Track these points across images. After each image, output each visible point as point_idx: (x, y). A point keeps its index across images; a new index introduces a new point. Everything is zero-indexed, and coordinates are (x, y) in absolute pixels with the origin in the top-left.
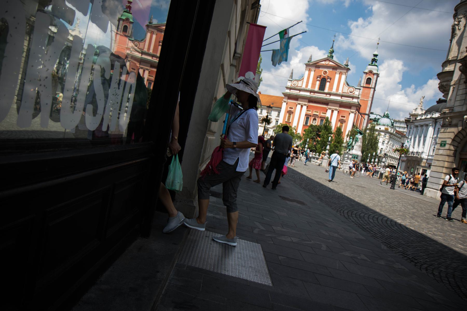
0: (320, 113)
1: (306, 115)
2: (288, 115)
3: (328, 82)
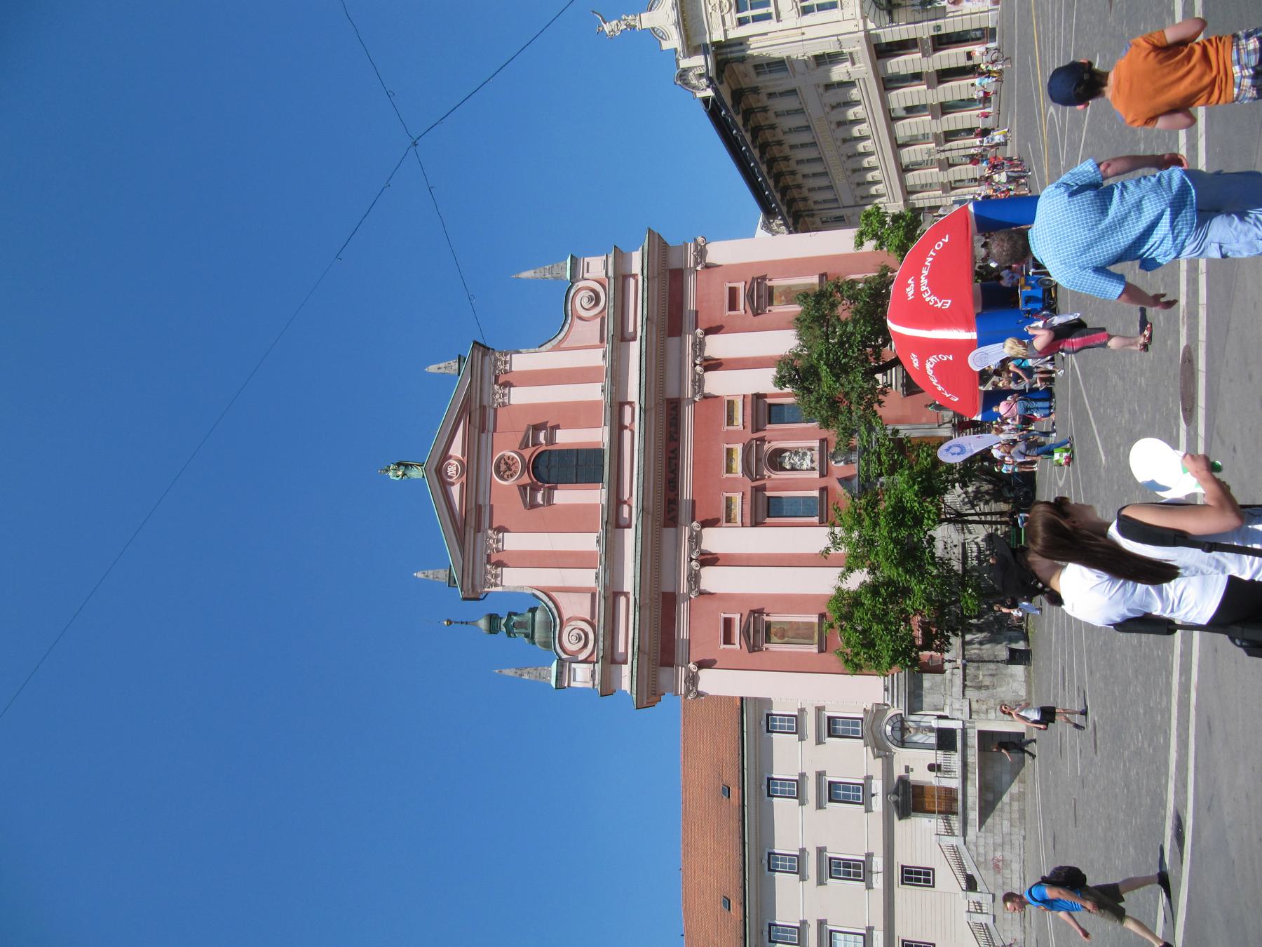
0: (730, 438)
1: (756, 523)
2: (776, 647)
3: (551, 440)
